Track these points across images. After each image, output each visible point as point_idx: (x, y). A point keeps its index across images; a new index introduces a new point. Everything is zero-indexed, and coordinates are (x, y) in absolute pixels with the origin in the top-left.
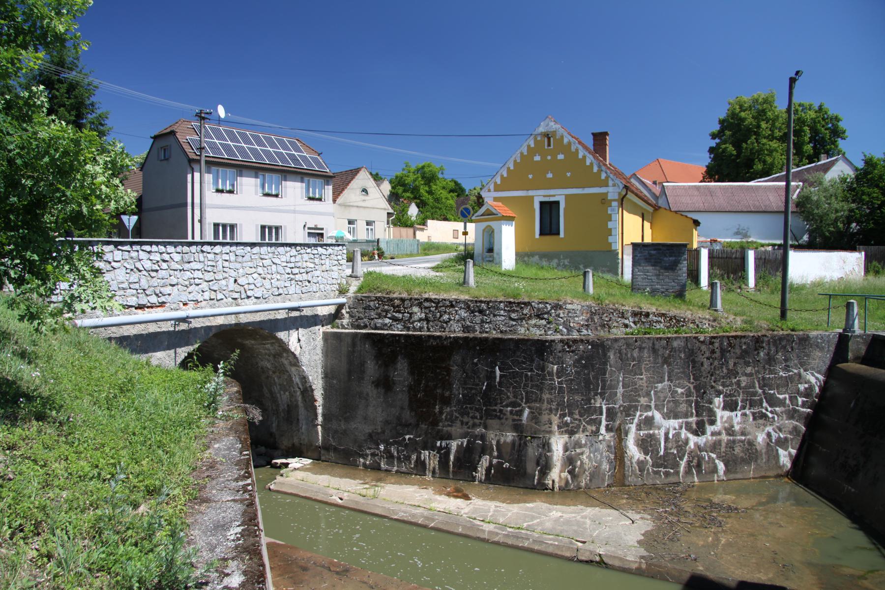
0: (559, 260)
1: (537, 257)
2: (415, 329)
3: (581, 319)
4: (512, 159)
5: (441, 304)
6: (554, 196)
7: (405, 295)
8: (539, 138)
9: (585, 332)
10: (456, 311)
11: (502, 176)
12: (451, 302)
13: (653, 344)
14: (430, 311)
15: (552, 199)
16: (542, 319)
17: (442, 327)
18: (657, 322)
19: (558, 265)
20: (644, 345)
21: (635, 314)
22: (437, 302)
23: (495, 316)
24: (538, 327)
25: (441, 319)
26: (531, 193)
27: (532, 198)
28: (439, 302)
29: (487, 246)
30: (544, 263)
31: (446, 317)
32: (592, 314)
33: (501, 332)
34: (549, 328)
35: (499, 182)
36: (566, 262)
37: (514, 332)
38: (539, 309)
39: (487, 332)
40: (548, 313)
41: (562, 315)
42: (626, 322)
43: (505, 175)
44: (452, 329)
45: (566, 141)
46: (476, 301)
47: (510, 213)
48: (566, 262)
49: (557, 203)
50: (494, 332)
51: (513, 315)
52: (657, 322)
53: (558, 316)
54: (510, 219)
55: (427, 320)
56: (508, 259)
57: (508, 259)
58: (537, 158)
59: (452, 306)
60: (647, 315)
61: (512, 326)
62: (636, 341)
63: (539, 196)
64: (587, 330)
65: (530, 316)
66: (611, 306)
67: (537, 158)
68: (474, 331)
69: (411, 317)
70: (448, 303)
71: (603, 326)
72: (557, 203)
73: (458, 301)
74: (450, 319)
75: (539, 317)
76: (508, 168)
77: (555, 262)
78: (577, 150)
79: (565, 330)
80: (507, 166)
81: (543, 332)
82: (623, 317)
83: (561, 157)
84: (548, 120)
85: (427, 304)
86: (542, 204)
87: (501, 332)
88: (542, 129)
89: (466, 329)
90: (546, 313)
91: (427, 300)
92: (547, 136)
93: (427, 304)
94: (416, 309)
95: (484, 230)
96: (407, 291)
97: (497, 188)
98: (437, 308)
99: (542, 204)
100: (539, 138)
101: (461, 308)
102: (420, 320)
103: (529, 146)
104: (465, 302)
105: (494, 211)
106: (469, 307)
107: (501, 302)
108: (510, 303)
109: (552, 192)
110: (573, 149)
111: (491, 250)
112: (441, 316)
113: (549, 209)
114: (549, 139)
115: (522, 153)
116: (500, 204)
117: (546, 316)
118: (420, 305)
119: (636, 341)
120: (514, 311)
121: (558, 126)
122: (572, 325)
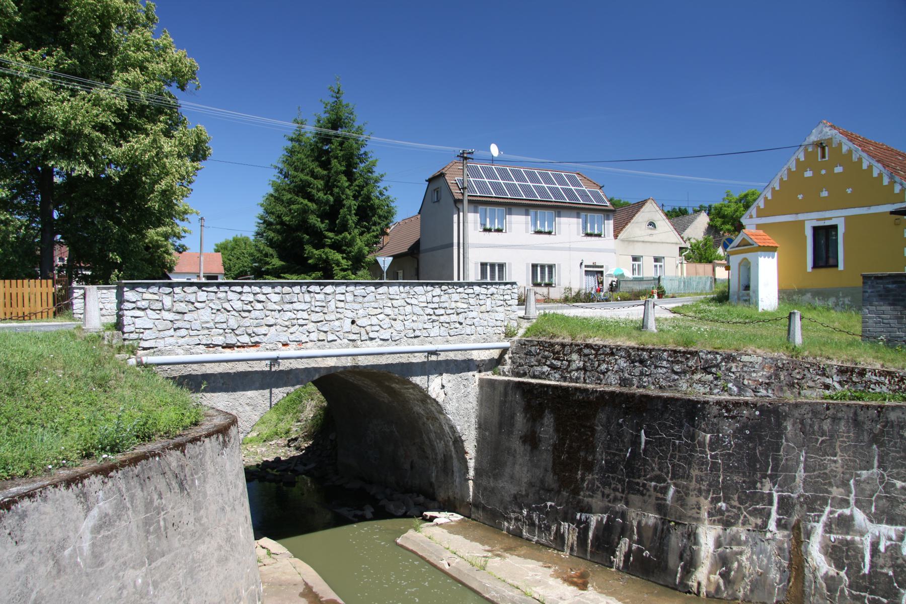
0: (837, 298)
1: (809, 295)
2: (572, 380)
3: (760, 376)
4: (778, 177)
5: (601, 352)
6: (830, 219)
7: (568, 340)
8: (810, 150)
9: (763, 392)
10: (616, 360)
11: (766, 198)
12: (611, 349)
13: (855, 414)
14: (589, 359)
15: (828, 223)
16: (710, 373)
17: (598, 378)
18: (878, 383)
19: (837, 305)
20: (840, 415)
21: (842, 371)
22: (597, 349)
23: (656, 367)
24: (703, 383)
25: (599, 370)
26: (801, 217)
27: (802, 223)
28: (599, 349)
29: (743, 282)
30: (817, 302)
31: (604, 367)
32: (778, 368)
33: (660, 387)
34: (716, 385)
35: (762, 206)
36: (847, 300)
37: (674, 387)
38: (706, 361)
39: (644, 387)
40: (718, 366)
41: (734, 370)
42: (828, 381)
43: (769, 198)
44: (609, 381)
45: (845, 149)
46: (638, 349)
47: (772, 243)
48: (847, 300)
49: (835, 228)
50: (653, 387)
51: (677, 368)
52: (878, 383)
53: (729, 370)
54: (769, 250)
55: (584, 369)
56: (768, 296)
57: (768, 296)
58: (808, 174)
59: (612, 354)
60: (862, 373)
61: (674, 380)
62: (828, 408)
63: (811, 220)
64: (767, 389)
65: (696, 369)
66: (810, 359)
67: (808, 174)
68: (632, 385)
69: (569, 366)
70: (608, 350)
71: (791, 385)
72: (835, 228)
73: (619, 348)
74: (608, 370)
75: (706, 370)
76: (773, 189)
77: (831, 302)
78: (860, 159)
79: (735, 389)
80: (771, 186)
81: (708, 390)
82: (824, 375)
83: (838, 169)
84: (821, 125)
85: (586, 351)
86: (816, 230)
87: (660, 387)
88: (814, 137)
89: (624, 382)
90: (714, 366)
91: (588, 346)
92: (821, 145)
93: (586, 351)
94: (575, 356)
95: (740, 264)
96: (571, 335)
97: (761, 214)
98: (596, 355)
99: (816, 230)
100: (810, 150)
101: (621, 357)
102: (578, 369)
103: (798, 160)
104: (627, 350)
105: (750, 241)
106: (629, 356)
107: (665, 351)
108: (675, 352)
109: (827, 214)
110: (855, 158)
111: (747, 288)
112: (599, 365)
113: (824, 237)
114: (823, 149)
115: (789, 170)
116: (761, 232)
117: (714, 370)
118: (579, 352)
119: (828, 408)
120: (678, 362)
121: (834, 132)
122: (746, 382)
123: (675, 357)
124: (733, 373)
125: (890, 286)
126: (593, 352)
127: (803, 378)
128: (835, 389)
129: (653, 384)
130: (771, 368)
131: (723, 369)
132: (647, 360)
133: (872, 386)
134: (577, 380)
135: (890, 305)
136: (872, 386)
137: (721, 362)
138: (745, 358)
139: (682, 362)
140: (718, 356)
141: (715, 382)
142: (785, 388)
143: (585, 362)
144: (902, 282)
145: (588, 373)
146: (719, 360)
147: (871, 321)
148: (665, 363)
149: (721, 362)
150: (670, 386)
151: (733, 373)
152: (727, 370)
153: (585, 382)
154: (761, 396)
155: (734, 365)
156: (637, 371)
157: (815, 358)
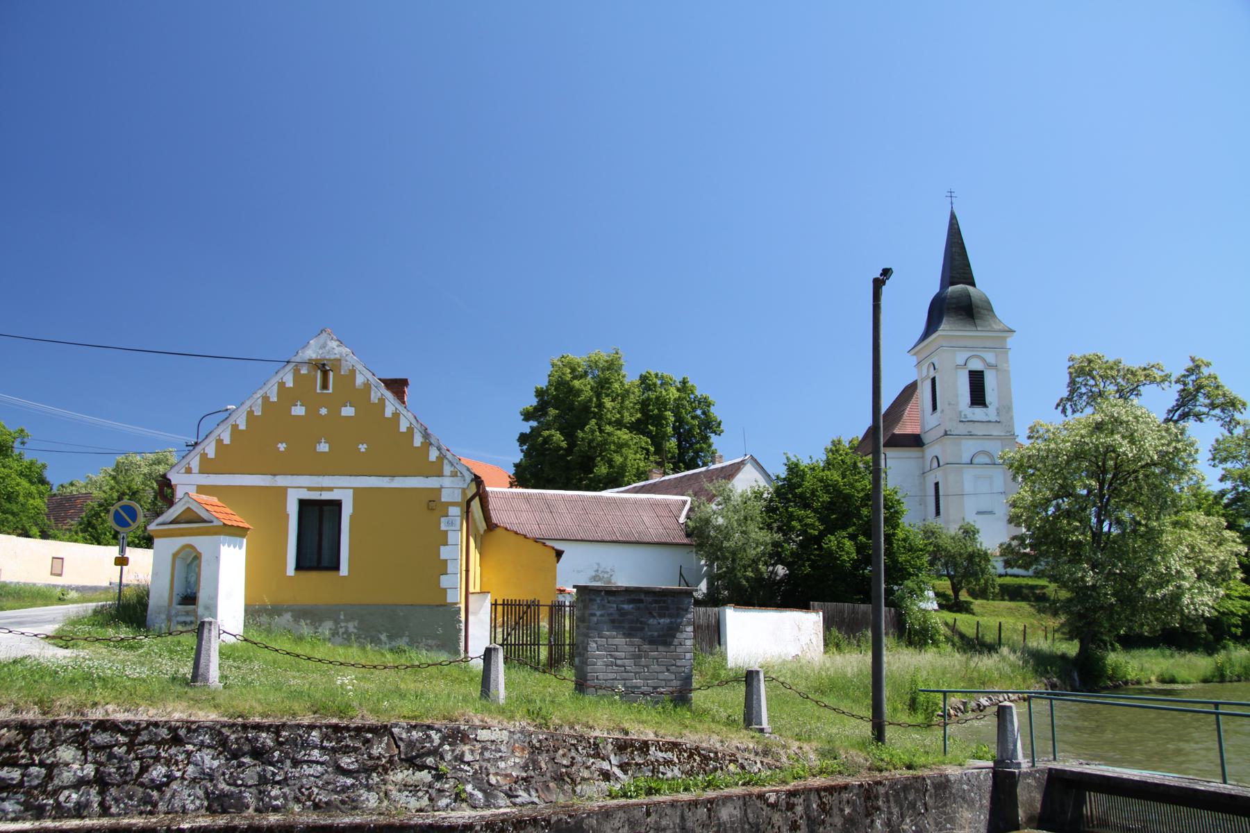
0: (337, 622)
1: (288, 616)
2: (60, 812)
3: (512, 764)
4: (246, 407)
5: (144, 736)
6: (331, 489)
7: (32, 715)
8: (304, 371)
9: (523, 797)
10: (189, 754)
11: (219, 442)
12: (173, 730)
13: (683, 818)
14: (111, 756)
15: (326, 496)
16: (422, 768)
17: (147, 800)
18: (668, 763)
19: (334, 633)
20: (664, 823)
21: (621, 747)
22: (133, 732)
23: (296, 763)
24: (413, 789)
25: (145, 778)
26: (281, 481)
27: (283, 491)
28: (138, 732)
29: (179, 589)
30: (305, 629)
31: (158, 772)
32: (535, 750)
33: (316, 806)
34: (440, 791)
35: (211, 454)
36: (352, 627)
37: (354, 805)
38: (411, 744)
39: (276, 809)
40: (435, 752)
41: (468, 757)
42: (605, 765)
43: (227, 441)
44: (177, 803)
45: (360, 380)
46: (245, 727)
47: (237, 520)
48: (352, 627)
49: (337, 504)
50: (297, 808)
51: (346, 761)
52: (668, 763)
53: (460, 758)
54: (237, 532)
55: (101, 782)
58: (299, 410)
59: (176, 740)
60: (644, 747)
61: (345, 789)
62: (648, 814)
63: (299, 487)
64: (527, 790)
65: (391, 761)
66: (567, 730)
67: (299, 410)
68: (241, 807)
69: (49, 777)
70: (164, 733)
71: (559, 778)
72: (337, 504)
73: (193, 728)
74: (170, 778)
75: (413, 762)
76: (235, 427)
77: (326, 628)
78: (382, 401)
79: (480, 795)
80: (231, 421)
81: (425, 802)
82: (597, 755)
83: (348, 411)
84: (324, 335)
85: (101, 738)
86: (303, 504)
87: (316, 806)
88: (311, 353)
89: (217, 803)
90: (430, 753)
91: (102, 726)
92: (323, 367)
93: (101, 738)
94: (66, 753)
95: (175, 556)
96: (40, 703)
97: (207, 467)
98: (131, 746)
99: (303, 504)
100: (304, 371)
101: (202, 746)
102: (79, 784)
103: (282, 385)
104: (214, 730)
105: (204, 515)
106: (224, 742)
107: (311, 727)
108: (336, 728)
109: (326, 481)
110: (374, 397)
111: (189, 599)
112: (144, 769)
113: (319, 518)
114: (325, 374)
115: (266, 398)
116: (215, 500)
117: (430, 761)
118: (81, 740)
119: (648, 814)
120: (347, 750)
121: (345, 350)
122: (493, 780)
123: (339, 741)
124: (468, 763)
125: (625, 606)
126: (122, 739)
127: (572, 764)
128: (617, 779)
129: (297, 800)
130: (523, 749)
131: (448, 757)
132: (272, 750)
133: (661, 768)
134: (80, 811)
135: (626, 635)
136: (661, 768)
137: (441, 745)
138: (483, 735)
139: (355, 750)
140: (432, 733)
141: (438, 785)
142: (552, 785)
143: (98, 764)
144: (641, 601)
145: (113, 791)
146: (437, 742)
147: (600, 662)
148: (316, 752)
149: (441, 745)
150: (343, 802)
151: (468, 763)
152: (456, 758)
153: (105, 811)
154: (522, 805)
155: (466, 748)
156: (250, 774)
157: (572, 727)
